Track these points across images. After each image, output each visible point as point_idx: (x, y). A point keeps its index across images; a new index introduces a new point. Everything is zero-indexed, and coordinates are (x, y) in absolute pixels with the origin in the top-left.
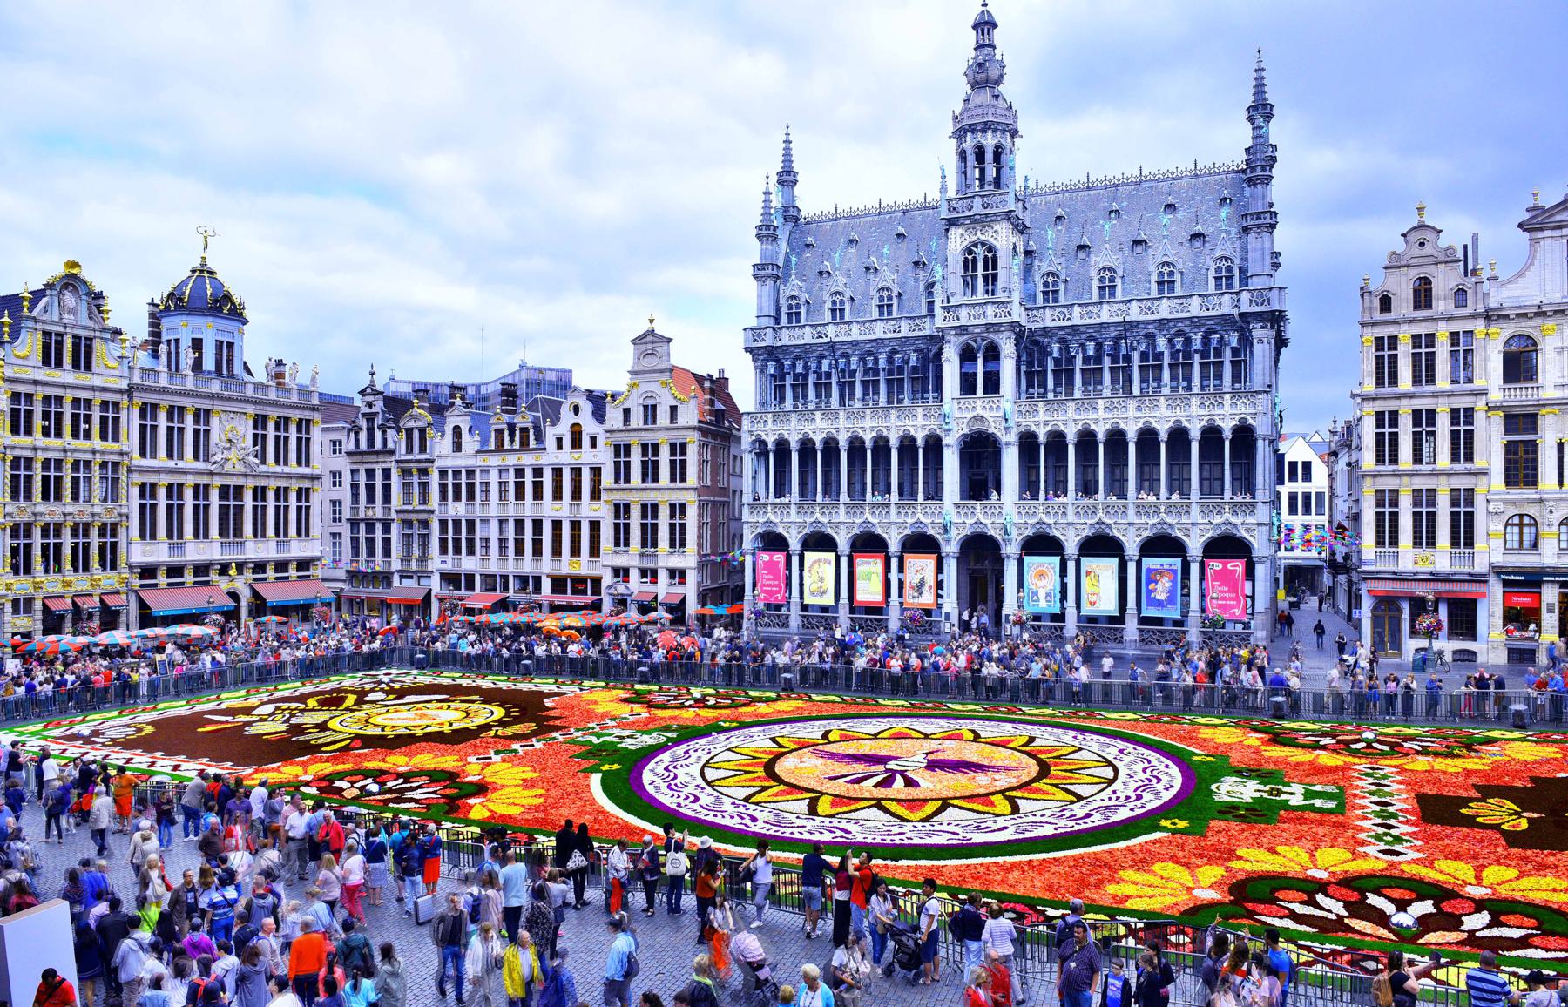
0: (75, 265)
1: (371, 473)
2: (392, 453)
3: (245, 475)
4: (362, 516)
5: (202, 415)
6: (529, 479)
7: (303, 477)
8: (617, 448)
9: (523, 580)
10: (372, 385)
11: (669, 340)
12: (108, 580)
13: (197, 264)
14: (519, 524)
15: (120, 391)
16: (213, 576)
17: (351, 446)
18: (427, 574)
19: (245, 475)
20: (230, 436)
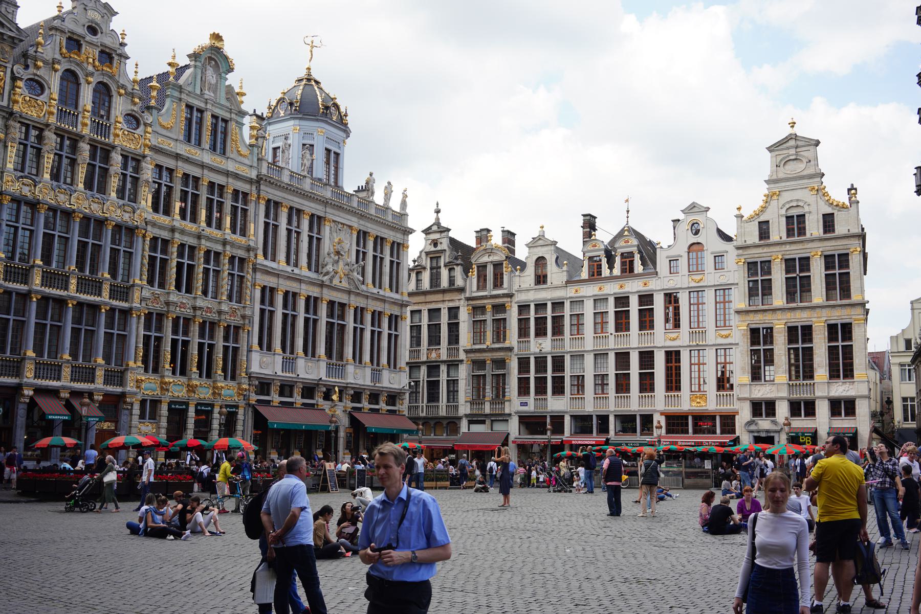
0: (217, 37)
1: (434, 313)
2: (462, 290)
3: (349, 292)
4: (424, 358)
5: (317, 221)
6: (634, 307)
7: (394, 303)
8: (752, 266)
9: (627, 422)
10: (437, 223)
11: (817, 143)
12: (229, 391)
13: (303, 74)
14: (623, 358)
15: (250, 181)
16: (319, 400)
17: (412, 287)
18: (504, 418)
19: (349, 292)
20: (338, 247)
